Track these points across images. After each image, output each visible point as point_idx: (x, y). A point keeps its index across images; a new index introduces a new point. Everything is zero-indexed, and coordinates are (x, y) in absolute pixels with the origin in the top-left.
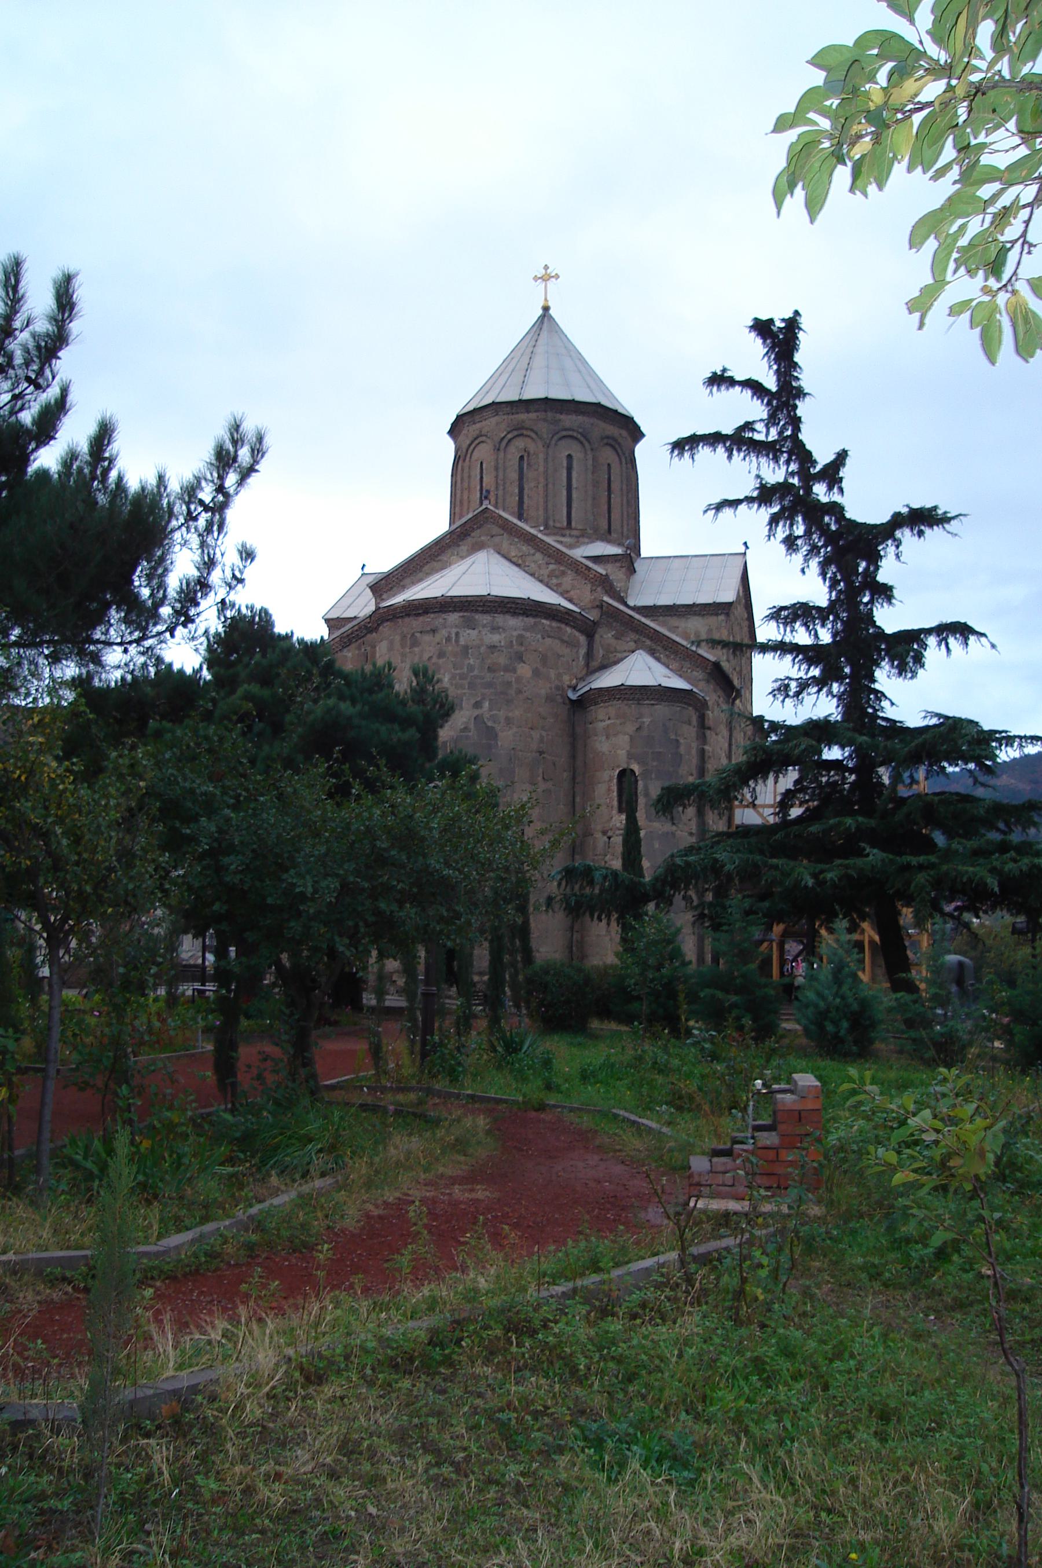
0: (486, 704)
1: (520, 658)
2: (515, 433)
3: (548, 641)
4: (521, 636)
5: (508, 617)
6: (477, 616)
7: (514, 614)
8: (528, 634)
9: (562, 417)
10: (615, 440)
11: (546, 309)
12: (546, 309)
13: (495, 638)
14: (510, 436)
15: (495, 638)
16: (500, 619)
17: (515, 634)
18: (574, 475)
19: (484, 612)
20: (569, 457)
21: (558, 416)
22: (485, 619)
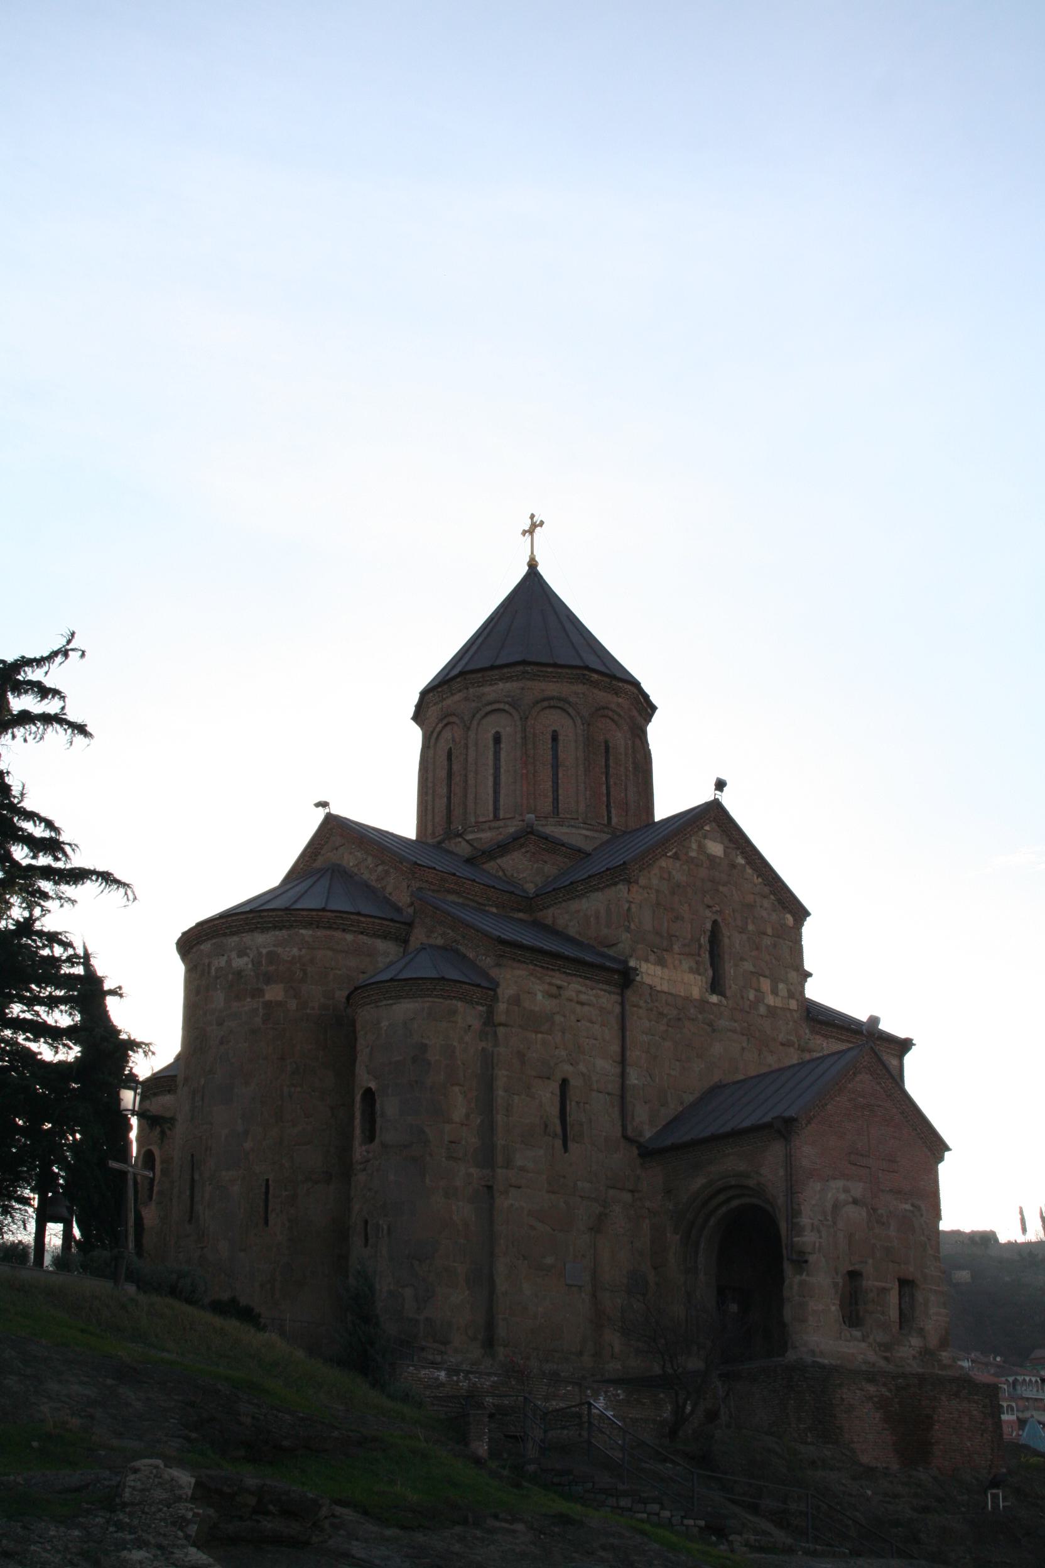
2: (445, 722)
4: (269, 953)
5: (256, 934)
7: (264, 930)
11: (532, 565)
12: (532, 565)
14: (438, 729)
16: (247, 938)
18: (503, 755)
19: (233, 934)
22: (233, 941)
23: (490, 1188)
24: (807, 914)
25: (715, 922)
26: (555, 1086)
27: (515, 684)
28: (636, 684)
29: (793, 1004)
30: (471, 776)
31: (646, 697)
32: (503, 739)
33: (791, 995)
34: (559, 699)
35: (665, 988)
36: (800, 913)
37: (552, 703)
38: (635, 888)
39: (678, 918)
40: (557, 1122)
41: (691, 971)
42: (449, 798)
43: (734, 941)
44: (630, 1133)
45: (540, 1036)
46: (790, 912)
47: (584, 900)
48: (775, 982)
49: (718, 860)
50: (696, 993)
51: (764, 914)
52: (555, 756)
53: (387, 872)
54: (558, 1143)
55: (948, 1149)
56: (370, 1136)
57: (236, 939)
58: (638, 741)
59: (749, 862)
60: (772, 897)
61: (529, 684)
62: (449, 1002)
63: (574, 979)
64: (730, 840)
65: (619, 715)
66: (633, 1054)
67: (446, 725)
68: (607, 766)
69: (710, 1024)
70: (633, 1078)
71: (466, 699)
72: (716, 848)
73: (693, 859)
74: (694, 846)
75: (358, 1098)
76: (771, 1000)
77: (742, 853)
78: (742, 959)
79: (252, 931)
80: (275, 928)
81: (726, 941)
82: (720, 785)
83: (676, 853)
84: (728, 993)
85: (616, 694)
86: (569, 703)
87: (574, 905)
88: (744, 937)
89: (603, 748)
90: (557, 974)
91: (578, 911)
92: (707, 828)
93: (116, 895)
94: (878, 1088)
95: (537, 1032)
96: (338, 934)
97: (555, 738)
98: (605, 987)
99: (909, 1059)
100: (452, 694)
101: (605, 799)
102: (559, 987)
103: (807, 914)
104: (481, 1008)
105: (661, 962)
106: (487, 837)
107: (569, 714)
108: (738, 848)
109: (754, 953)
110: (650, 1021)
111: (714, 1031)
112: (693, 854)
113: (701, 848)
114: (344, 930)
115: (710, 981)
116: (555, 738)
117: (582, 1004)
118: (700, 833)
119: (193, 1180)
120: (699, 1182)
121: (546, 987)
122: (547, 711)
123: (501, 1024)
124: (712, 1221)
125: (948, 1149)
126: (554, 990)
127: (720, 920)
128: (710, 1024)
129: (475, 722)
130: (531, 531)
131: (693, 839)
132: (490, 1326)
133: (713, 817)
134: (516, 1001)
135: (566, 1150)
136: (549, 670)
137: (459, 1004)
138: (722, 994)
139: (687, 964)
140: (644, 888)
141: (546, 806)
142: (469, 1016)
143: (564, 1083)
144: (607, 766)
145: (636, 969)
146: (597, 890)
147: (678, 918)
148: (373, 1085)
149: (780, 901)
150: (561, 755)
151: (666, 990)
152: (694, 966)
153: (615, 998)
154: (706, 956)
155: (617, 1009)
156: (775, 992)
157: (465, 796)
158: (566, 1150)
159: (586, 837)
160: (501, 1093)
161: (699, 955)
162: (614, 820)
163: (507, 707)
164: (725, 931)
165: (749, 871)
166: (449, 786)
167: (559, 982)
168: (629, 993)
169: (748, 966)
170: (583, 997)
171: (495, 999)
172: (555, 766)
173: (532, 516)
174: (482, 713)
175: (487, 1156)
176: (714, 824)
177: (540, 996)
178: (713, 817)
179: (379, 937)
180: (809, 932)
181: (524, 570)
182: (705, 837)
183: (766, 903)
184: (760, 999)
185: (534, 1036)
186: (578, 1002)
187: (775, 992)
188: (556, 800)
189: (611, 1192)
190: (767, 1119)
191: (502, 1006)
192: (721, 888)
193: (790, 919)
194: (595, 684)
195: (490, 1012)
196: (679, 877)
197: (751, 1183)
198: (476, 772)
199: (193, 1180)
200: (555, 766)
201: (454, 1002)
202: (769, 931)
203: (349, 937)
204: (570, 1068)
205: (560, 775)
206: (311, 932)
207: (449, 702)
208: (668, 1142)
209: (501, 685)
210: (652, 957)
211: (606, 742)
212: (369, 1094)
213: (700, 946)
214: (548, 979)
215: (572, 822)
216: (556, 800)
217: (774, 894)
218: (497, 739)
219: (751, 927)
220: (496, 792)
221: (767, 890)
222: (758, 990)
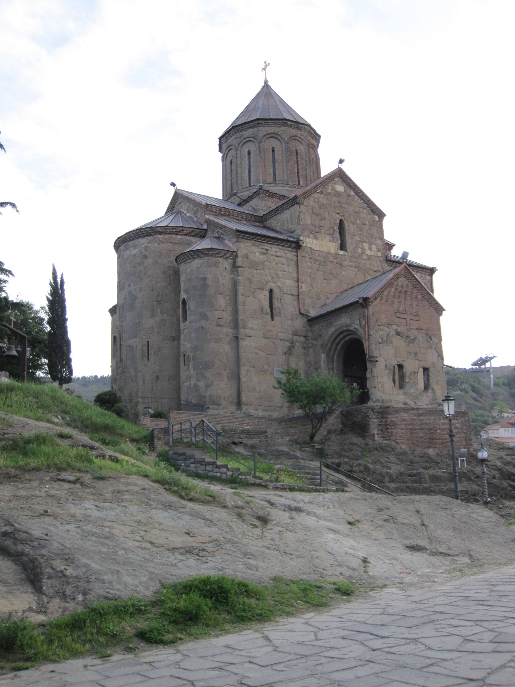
0: (132, 285)
1: (146, 257)
2: (228, 149)
3: (162, 245)
4: (146, 246)
6: (128, 243)
7: (143, 237)
8: (150, 245)
9: (244, 133)
10: (277, 134)
11: (266, 82)
12: (266, 82)
13: (135, 251)
15: (135, 251)
16: (136, 241)
17: (144, 246)
18: (252, 159)
19: (131, 240)
21: (241, 134)
22: (131, 243)
23: (237, 337)
25: (341, 221)
26: (267, 293)
27: (255, 129)
28: (309, 126)
30: (239, 169)
31: (314, 131)
32: (251, 153)
34: (274, 134)
36: (381, 215)
37: (271, 135)
38: (302, 206)
40: (268, 308)
41: (330, 241)
42: (232, 181)
43: (349, 228)
44: (302, 312)
45: (258, 271)
46: (377, 215)
47: (282, 214)
48: (370, 244)
49: (341, 194)
50: (333, 251)
51: (365, 216)
53: (197, 209)
54: (269, 317)
55: (444, 310)
57: (132, 242)
58: (311, 150)
60: (368, 209)
61: (261, 128)
62: (215, 258)
63: (274, 246)
64: (347, 185)
65: (301, 139)
66: (302, 278)
67: (229, 150)
70: (304, 288)
71: (236, 138)
72: (340, 188)
73: (329, 193)
74: (330, 188)
75: (181, 303)
76: (368, 252)
77: (353, 190)
78: (354, 236)
79: (138, 238)
80: (148, 236)
81: (346, 228)
82: (341, 161)
83: (321, 191)
84: (348, 250)
85: (300, 130)
86: (278, 135)
87: (278, 217)
88: (355, 226)
89: (295, 153)
90: (266, 244)
91: (280, 219)
92: (336, 180)
94: (409, 284)
95: (256, 270)
96: (174, 236)
97: (273, 151)
98: (289, 249)
99: (435, 276)
100: (231, 137)
101: (297, 174)
102: (267, 250)
104: (230, 260)
105: (315, 238)
106: (246, 194)
107: (279, 140)
108: (351, 188)
109: (360, 233)
110: (311, 263)
111: (342, 266)
112: (329, 191)
113: (333, 189)
114: (177, 234)
115: (339, 245)
116: (273, 151)
117: (278, 257)
118: (333, 182)
119: (121, 344)
120: (332, 329)
121: (261, 250)
122: (270, 139)
123: (239, 267)
124: (339, 346)
125: (444, 310)
126: (264, 251)
127: (343, 219)
128: (340, 264)
129: (240, 147)
130: (264, 69)
131: (329, 184)
132: (239, 397)
133: (340, 175)
134: (246, 256)
135: (273, 320)
136: (269, 121)
137: (220, 259)
138: (346, 251)
139: (328, 238)
140: (306, 206)
141: (270, 178)
142: (226, 264)
143: (271, 291)
145: (302, 241)
146: (287, 209)
148: (185, 297)
149: (372, 210)
150: (276, 157)
151: (318, 249)
152: (331, 239)
154: (338, 235)
156: (370, 249)
157: (237, 178)
158: (273, 320)
159: (288, 190)
161: (334, 234)
162: (301, 183)
163: (252, 139)
164: (346, 223)
165: (356, 197)
166: (231, 175)
167: (266, 248)
169: (357, 238)
170: (278, 254)
171: (236, 256)
172: (274, 162)
173: (265, 62)
174: (242, 143)
175: (236, 324)
176: (339, 178)
177: (257, 254)
178: (340, 175)
179: (192, 236)
180: (386, 222)
181: (263, 84)
182: (335, 184)
183: (365, 211)
184: (363, 253)
185: (255, 271)
186: (276, 256)
187: (370, 249)
188: (275, 176)
189: (295, 337)
191: (239, 259)
192: (343, 205)
193: (377, 218)
194: (290, 126)
195: (235, 262)
196: (323, 201)
197: (352, 328)
198: (241, 168)
199: (121, 344)
200: (274, 162)
201: (218, 258)
202: (367, 223)
203: (179, 237)
204: (273, 285)
205: (276, 165)
206: (162, 236)
207: (229, 140)
209: (250, 130)
210: (312, 236)
211: (297, 150)
212: (184, 302)
213: (334, 230)
214: (262, 247)
215: (282, 185)
216: (275, 176)
217: (369, 207)
218: (249, 153)
219: (358, 222)
220: (250, 175)
221: (365, 206)
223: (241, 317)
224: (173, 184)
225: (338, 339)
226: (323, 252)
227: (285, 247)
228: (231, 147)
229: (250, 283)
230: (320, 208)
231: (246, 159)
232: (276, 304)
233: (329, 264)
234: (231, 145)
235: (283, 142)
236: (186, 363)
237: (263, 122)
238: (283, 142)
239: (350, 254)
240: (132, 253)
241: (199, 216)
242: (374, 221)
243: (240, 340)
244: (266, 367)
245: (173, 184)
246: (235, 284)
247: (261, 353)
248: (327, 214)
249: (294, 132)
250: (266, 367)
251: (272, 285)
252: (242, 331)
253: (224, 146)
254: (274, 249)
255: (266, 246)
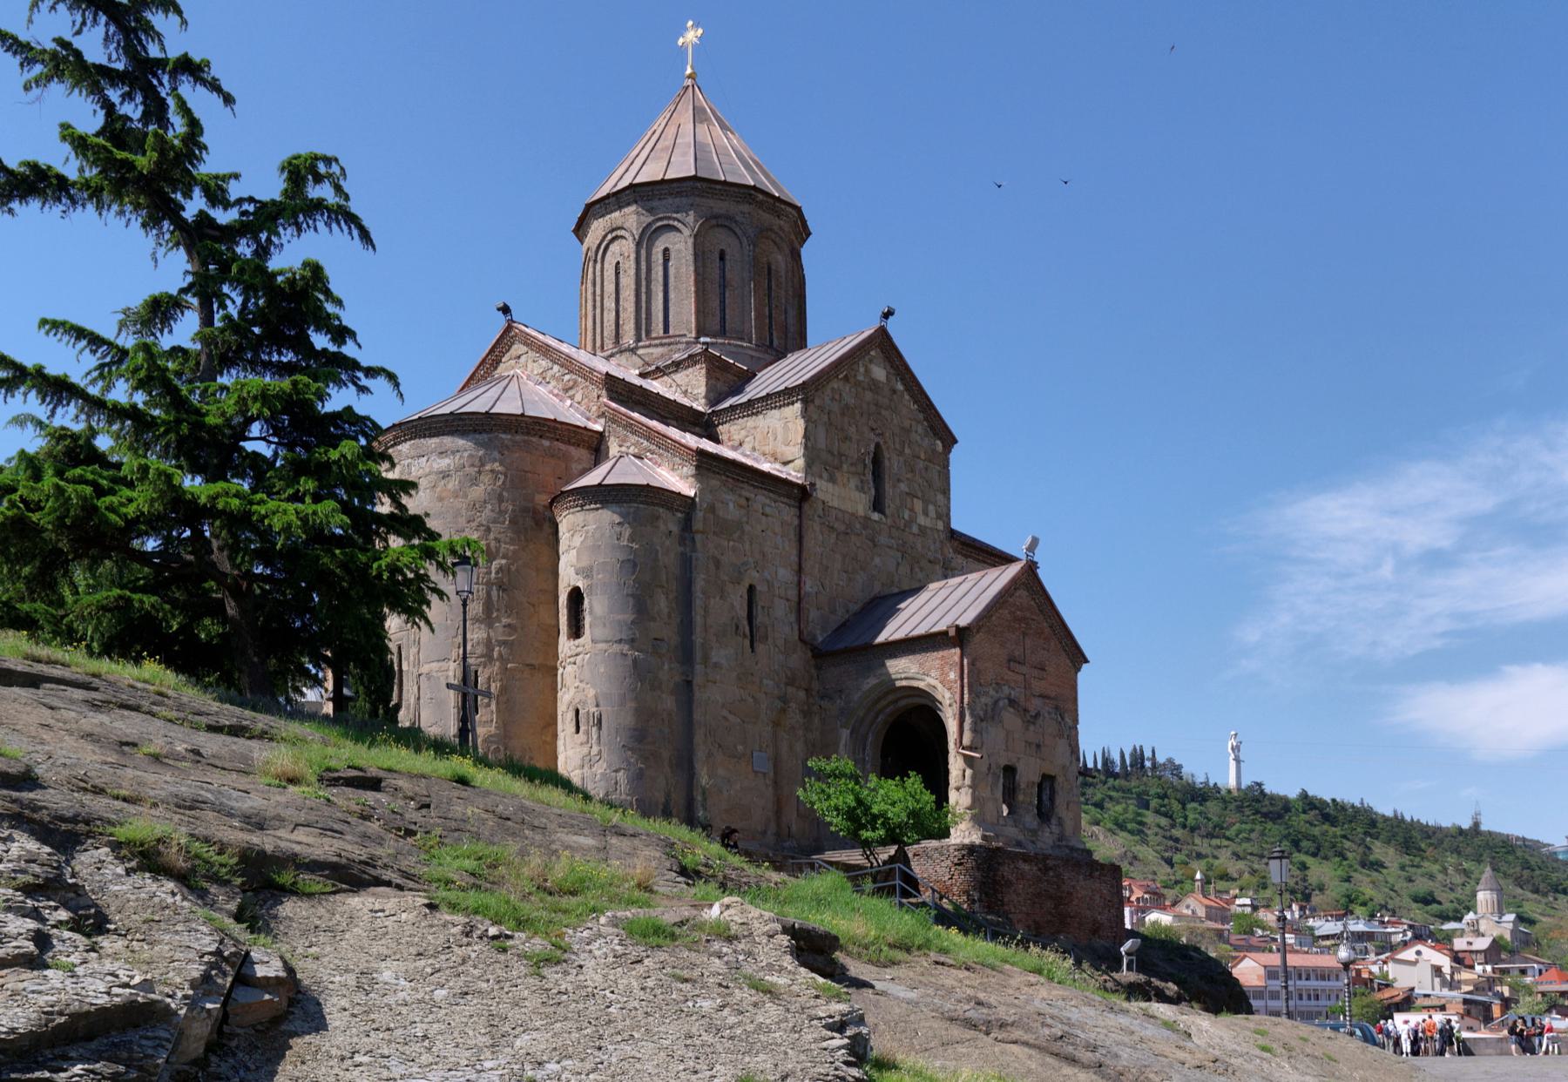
10: (731, 218)
13: (444, 463)
15: (444, 463)
20: (666, 250)
24: (955, 441)
25: (878, 446)
28: (798, 209)
29: (940, 525)
33: (939, 517)
35: (835, 504)
36: (949, 440)
39: (847, 438)
40: (745, 622)
43: (892, 463)
48: (926, 502)
50: (861, 512)
52: (723, 277)
54: (747, 642)
56: (576, 631)
59: (907, 389)
66: (807, 566)
68: (770, 288)
69: (872, 541)
70: (809, 586)
72: (879, 373)
74: (862, 370)
76: (922, 520)
81: (887, 463)
82: (888, 315)
87: (750, 422)
93: (398, 401)
97: (722, 257)
103: (955, 441)
105: (832, 480)
106: (655, 354)
112: (861, 378)
113: (867, 371)
116: (722, 257)
133: (882, 343)
138: (882, 512)
143: (751, 589)
144: (770, 288)
147: (847, 438)
149: (932, 427)
153: (794, 511)
154: (869, 477)
155: (796, 522)
156: (926, 513)
160: (699, 594)
162: (776, 342)
164: (886, 455)
168: (806, 506)
169: (903, 487)
170: (768, 510)
172: (723, 286)
182: (871, 361)
184: (912, 520)
187: (926, 513)
188: (723, 319)
189: (790, 690)
190: (941, 627)
192: (883, 412)
197: (921, 685)
200: (723, 286)
203: (546, 443)
208: (841, 646)
216: (723, 319)
219: (907, 451)
221: (921, 416)
222: (912, 510)
223: (698, 638)
224: (505, 310)
225: (884, 703)
226: (843, 512)
227: (780, 495)
228: (619, 233)
229: (717, 567)
230: (843, 414)
231: (661, 268)
232: (760, 618)
233: (853, 538)
234: (621, 228)
235: (745, 240)
236: (582, 729)
237: (705, 185)
238: (745, 240)
239: (889, 521)
240: (435, 466)
241: (578, 397)
242: (934, 451)
243: (696, 688)
244: (740, 748)
245: (505, 310)
246: (687, 564)
247: (731, 717)
248: (853, 429)
249: (767, 218)
250: (740, 748)
251: (753, 576)
252: (699, 668)
253: (598, 228)
254: (761, 499)
255: (747, 491)
